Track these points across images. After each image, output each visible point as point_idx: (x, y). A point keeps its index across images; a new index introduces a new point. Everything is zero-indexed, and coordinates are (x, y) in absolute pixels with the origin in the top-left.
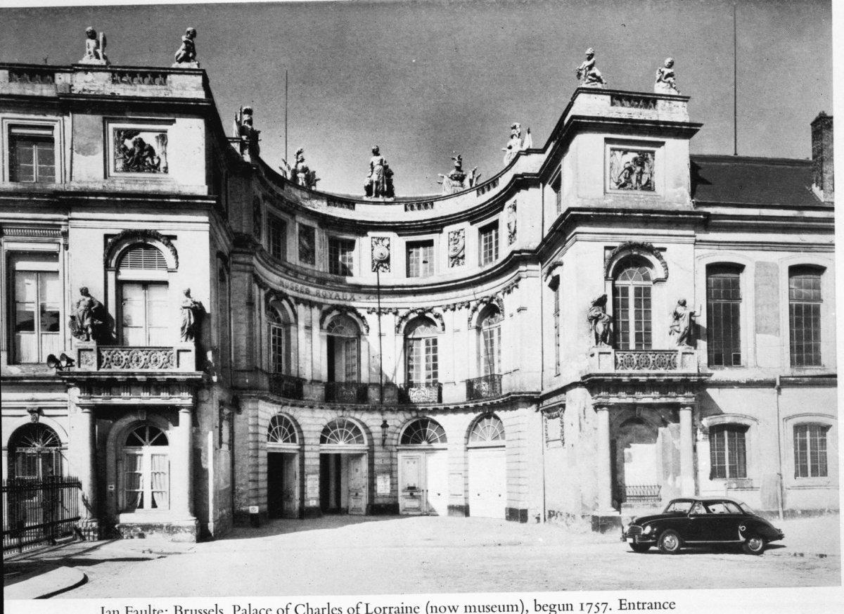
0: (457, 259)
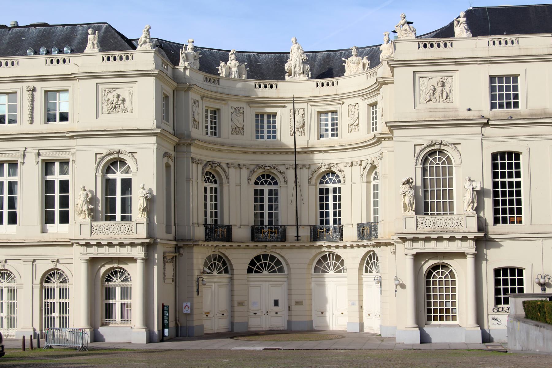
0: (354, 127)
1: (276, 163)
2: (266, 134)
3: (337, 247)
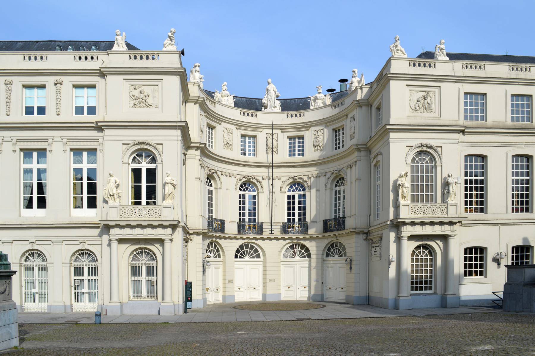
1: (255, 174)
2: (247, 152)
3: (305, 239)
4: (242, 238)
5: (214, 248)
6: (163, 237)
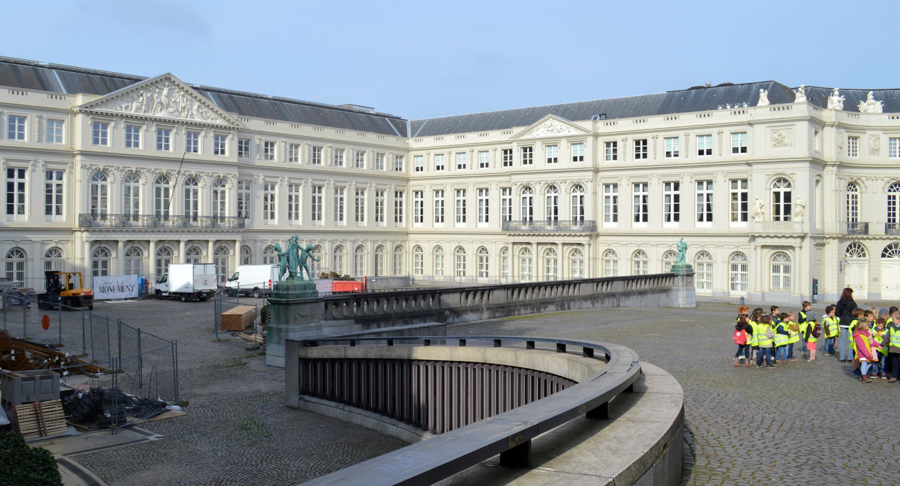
4: (888, 238)
5: (856, 249)
6: (794, 245)
